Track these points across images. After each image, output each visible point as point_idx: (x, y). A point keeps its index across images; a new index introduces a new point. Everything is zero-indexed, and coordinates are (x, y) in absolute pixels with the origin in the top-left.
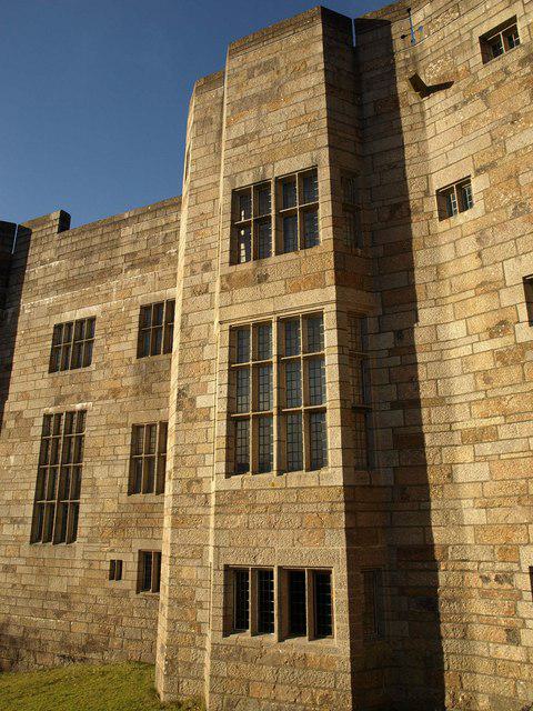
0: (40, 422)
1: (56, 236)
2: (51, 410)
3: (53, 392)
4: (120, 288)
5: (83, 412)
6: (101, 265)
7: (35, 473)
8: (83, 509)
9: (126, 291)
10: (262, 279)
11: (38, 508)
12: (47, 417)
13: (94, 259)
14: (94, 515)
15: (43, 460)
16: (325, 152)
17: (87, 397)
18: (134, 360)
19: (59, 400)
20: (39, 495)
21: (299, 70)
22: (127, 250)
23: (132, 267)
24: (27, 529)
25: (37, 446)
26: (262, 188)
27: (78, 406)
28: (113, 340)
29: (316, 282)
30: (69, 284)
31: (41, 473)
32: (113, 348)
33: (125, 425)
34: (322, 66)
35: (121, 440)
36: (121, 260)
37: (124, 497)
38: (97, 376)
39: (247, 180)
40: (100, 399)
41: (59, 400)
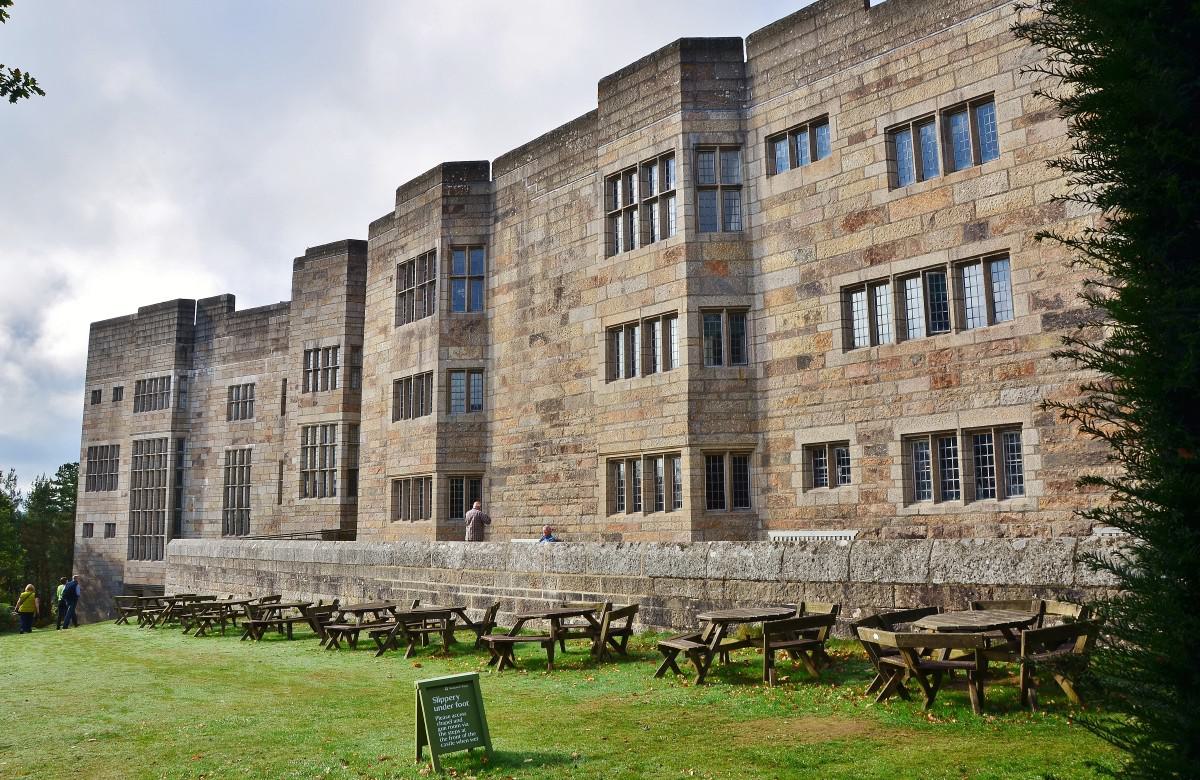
0: (223, 456)
1: (225, 316)
2: (230, 448)
3: (230, 435)
4: (270, 365)
5: (250, 450)
6: (256, 344)
7: (222, 490)
8: (253, 514)
9: (273, 367)
10: (315, 404)
11: (226, 513)
12: (228, 452)
13: (252, 339)
14: (259, 518)
15: (227, 482)
16: (343, 338)
17: (252, 441)
18: (280, 417)
19: (235, 441)
20: (226, 505)
21: (337, 283)
22: (273, 335)
23: (277, 350)
24: (219, 527)
25: (222, 471)
26: (317, 350)
27: (247, 447)
28: (266, 402)
29: (334, 410)
30: (237, 356)
31: (226, 490)
32: (267, 407)
33: (275, 461)
34: (346, 283)
35: (273, 471)
36: (269, 343)
37: (276, 506)
38: (258, 426)
39: (311, 346)
40: (260, 442)
41: (235, 441)
